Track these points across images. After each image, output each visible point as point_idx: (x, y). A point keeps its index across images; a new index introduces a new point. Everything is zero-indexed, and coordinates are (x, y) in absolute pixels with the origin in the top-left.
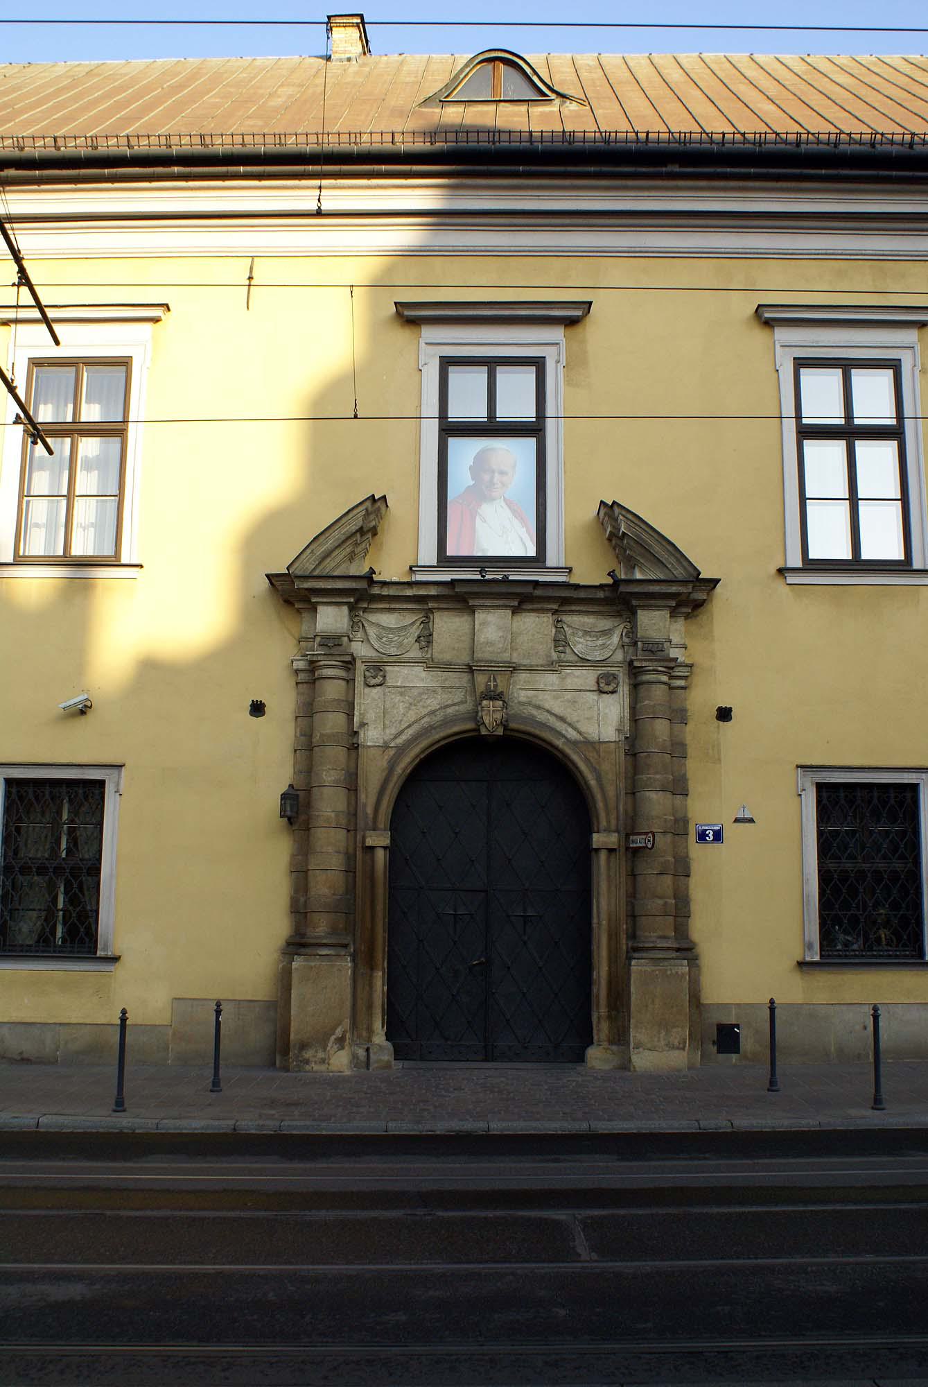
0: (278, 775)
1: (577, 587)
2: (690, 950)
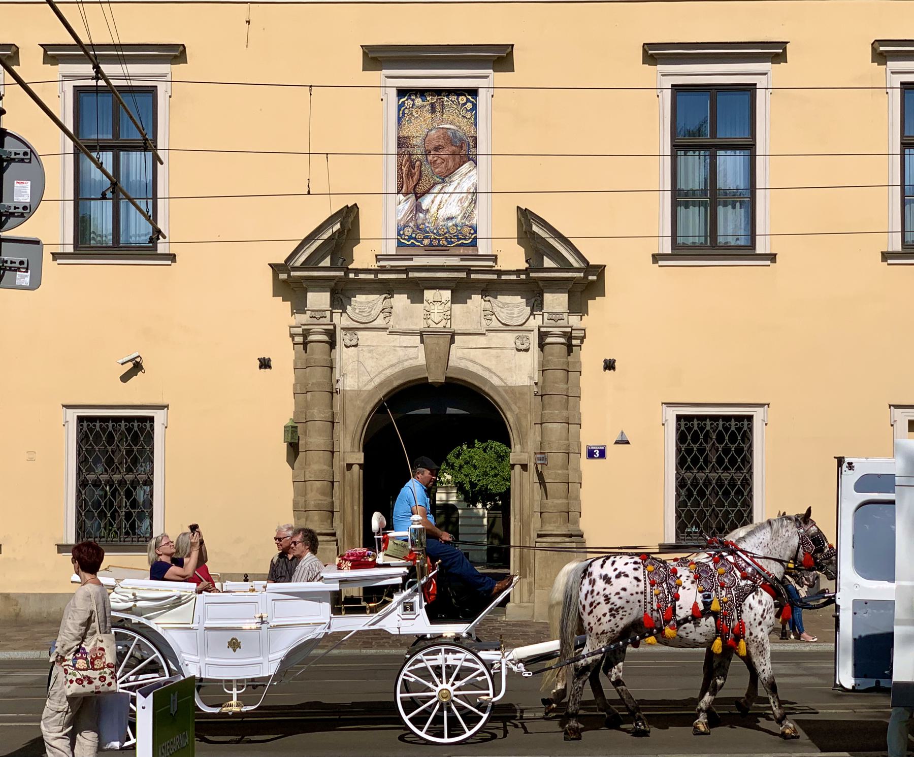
0: (285, 410)
1: (500, 273)
2: (582, 536)
